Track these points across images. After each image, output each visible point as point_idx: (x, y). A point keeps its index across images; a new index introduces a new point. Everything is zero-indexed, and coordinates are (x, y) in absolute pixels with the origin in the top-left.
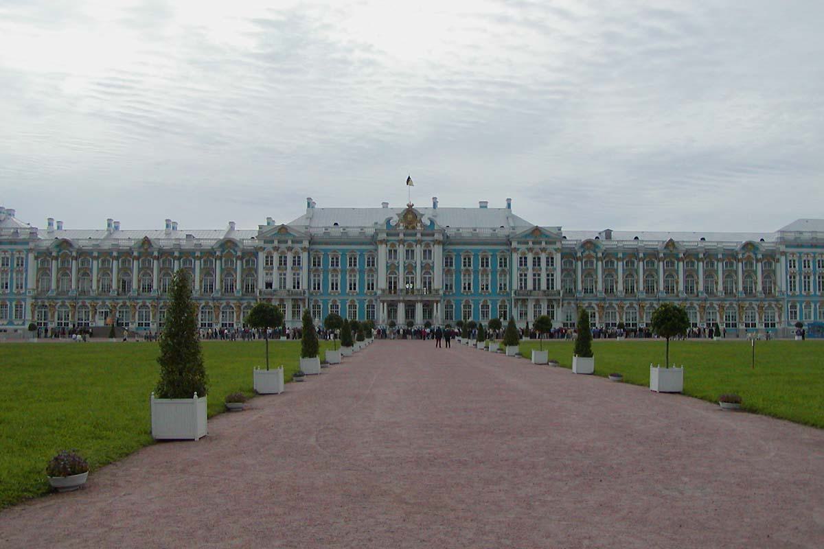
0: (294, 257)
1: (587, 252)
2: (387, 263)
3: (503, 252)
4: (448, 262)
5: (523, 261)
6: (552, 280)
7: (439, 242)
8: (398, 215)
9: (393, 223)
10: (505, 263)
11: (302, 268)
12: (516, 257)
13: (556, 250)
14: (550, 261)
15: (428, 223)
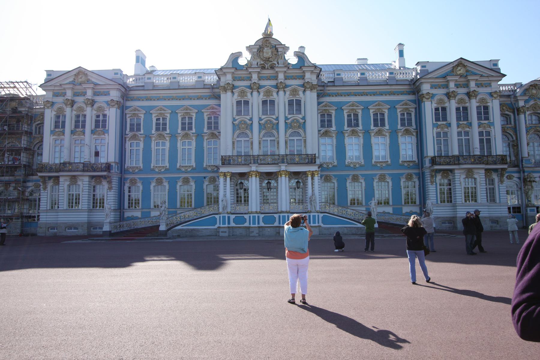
0: (98, 116)
1: (532, 102)
2: (234, 120)
3: (406, 104)
4: (325, 121)
5: (441, 114)
6: (489, 141)
7: (312, 88)
8: (249, 48)
9: (242, 61)
10: (410, 120)
11: (108, 131)
12: (429, 108)
13: (491, 95)
14: (484, 112)
15: (293, 60)
